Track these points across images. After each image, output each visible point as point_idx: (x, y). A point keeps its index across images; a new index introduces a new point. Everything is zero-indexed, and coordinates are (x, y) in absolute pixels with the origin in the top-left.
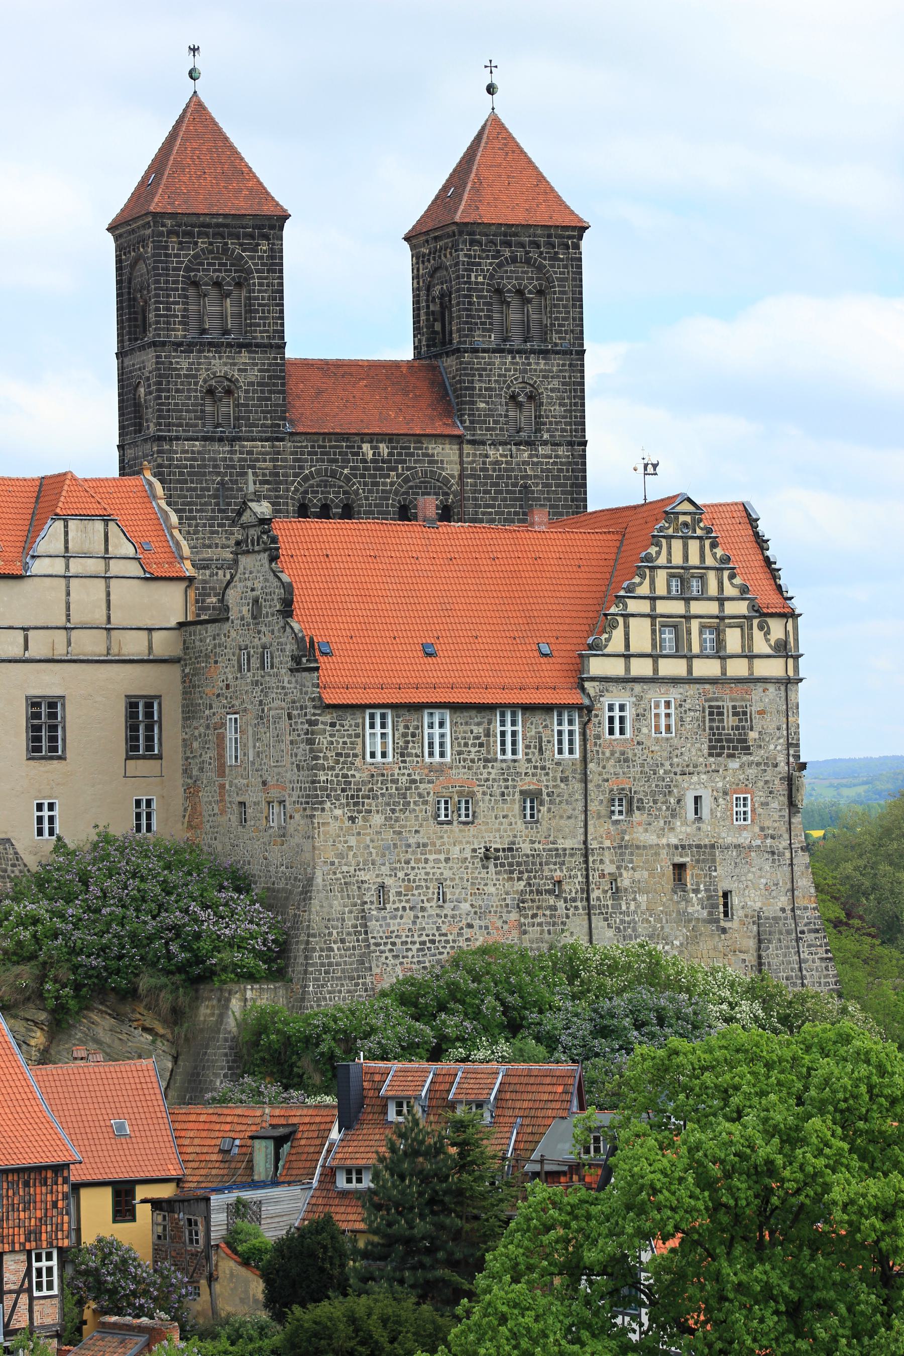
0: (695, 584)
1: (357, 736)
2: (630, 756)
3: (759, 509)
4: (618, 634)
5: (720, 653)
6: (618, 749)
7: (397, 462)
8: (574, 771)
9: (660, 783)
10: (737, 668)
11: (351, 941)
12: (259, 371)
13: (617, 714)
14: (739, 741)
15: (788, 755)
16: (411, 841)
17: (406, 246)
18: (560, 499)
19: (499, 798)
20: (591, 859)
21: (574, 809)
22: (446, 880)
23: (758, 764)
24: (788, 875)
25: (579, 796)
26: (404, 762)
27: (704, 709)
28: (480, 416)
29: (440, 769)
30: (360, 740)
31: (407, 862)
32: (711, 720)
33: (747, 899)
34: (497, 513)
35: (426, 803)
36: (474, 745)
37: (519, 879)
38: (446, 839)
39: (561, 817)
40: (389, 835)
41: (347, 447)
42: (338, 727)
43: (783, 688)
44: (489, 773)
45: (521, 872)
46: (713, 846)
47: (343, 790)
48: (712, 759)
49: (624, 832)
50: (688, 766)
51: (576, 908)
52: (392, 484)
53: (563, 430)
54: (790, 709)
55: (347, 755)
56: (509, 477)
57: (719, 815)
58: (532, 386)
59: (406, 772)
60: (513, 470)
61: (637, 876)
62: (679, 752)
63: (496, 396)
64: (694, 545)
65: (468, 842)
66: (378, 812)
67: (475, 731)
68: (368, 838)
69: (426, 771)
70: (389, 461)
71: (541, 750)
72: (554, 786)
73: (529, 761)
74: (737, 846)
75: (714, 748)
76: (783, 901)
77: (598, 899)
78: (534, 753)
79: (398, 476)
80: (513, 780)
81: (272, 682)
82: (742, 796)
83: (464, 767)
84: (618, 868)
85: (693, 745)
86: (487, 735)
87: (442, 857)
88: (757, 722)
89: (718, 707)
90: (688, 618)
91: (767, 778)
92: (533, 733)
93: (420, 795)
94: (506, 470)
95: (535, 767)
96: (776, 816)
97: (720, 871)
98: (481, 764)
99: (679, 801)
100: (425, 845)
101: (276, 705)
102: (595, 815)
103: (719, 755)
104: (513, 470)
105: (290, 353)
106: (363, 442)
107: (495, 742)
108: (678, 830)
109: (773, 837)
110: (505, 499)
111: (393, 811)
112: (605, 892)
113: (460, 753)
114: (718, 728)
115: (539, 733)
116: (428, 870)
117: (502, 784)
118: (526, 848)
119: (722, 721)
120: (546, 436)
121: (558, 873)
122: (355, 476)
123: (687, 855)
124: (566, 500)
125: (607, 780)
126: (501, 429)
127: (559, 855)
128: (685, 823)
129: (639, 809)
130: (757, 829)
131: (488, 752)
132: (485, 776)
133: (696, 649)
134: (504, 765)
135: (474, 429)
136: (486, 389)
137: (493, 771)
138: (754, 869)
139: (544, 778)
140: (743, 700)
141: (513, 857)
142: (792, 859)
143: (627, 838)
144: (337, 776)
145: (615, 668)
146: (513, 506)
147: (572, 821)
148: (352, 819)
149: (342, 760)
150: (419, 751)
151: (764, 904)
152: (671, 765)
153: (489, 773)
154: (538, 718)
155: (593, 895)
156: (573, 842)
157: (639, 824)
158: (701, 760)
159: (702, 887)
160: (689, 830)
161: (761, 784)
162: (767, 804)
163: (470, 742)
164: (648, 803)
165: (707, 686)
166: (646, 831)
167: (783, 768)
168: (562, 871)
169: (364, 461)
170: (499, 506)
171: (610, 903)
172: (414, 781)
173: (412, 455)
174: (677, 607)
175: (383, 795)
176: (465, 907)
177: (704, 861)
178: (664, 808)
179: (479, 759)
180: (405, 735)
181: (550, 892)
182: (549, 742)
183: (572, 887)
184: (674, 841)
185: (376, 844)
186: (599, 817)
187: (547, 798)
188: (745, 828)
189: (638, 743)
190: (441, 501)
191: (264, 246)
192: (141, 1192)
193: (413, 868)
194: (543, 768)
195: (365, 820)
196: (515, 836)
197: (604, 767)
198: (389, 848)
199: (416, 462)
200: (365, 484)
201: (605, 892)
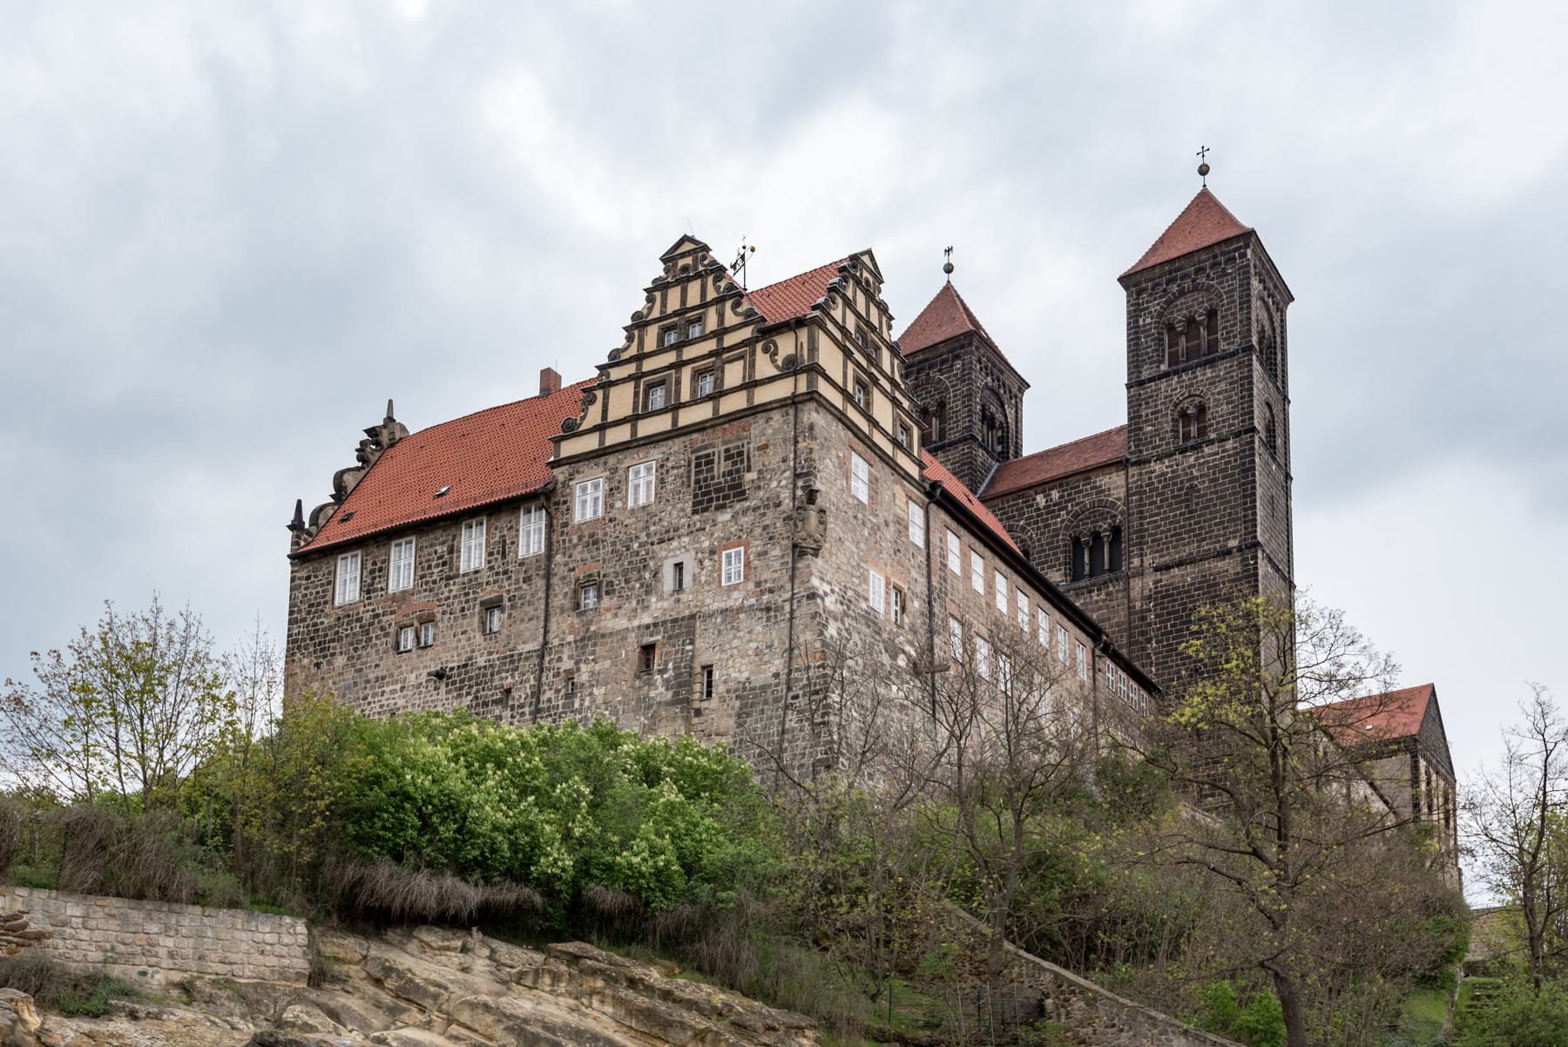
1: (329, 583)
2: (600, 536)
6: (586, 533)
7: (1066, 502)
8: (538, 568)
9: (633, 559)
12: (951, 464)
14: (731, 488)
15: (795, 487)
16: (371, 676)
18: (1227, 489)
19: (459, 614)
20: (547, 658)
21: (536, 610)
22: (398, 709)
23: (755, 509)
24: (786, 631)
25: (542, 594)
26: (369, 598)
27: (690, 462)
28: (1146, 438)
30: (330, 587)
31: (365, 698)
32: (697, 473)
33: (731, 671)
34: (1162, 520)
35: (387, 635)
36: (437, 566)
37: (468, 694)
38: (404, 668)
39: (522, 620)
40: (350, 675)
41: (1023, 503)
42: (312, 579)
43: (791, 412)
44: (451, 591)
45: (470, 687)
46: (693, 617)
47: (312, 639)
48: (697, 517)
49: (590, 623)
50: (667, 532)
51: (523, 714)
52: (1062, 522)
53: (1230, 426)
55: (319, 604)
56: (1174, 484)
57: (703, 579)
58: (1199, 396)
59: (370, 608)
60: (1178, 476)
61: (597, 667)
62: (657, 519)
63: (1162, 417)
65: (425, 667)
66: (341, 653)
67: (439, 551)
68: (331, 681)
69: (389, 603)
70: (1060, 503)
71: (504, 555)
72: (516, 589)
73: (491, 568)
74: (723, 612)
75: (701, 503)
76: (778, 664)
77: (549, 700)
78: (496, 559)
79: (1068, 514)
80: (474, 592)
82: (733, 551)
83: (426, 590)
84: (577, 663)
85: (674, 506)
86: (451, 551)
87: (398, 687)
88: (757, 462)
89: (708, 455)
91: (765, 523)
92: (497, 539)
93: (382, 629)
94: (1171, 478)
95: (497, 574)
96: (777, 565)
97: (699, 643)
98: (443, 583)
99: (655, 576)
100: (383, 678)
102: (558, 611)
103: (705, 510)
104: (1178, 476)
106: (1037, 494)
107: (459, 557)
108: (653, 607)
109: (771, 591)
110: (1171, 504)
111: (356, 650)
112: (558, 691)
113: (422, 577)
114: (706, 479)
115: (504, 536)
116: (384, 702)
117: (463, 599)
118: (481, 662)
119: (712, 470)
120: (1213, 436)
121: (510, 680)
122: (1029, 525)
123: (658, 633)
124: (1234, 487)
125: (573, 569)
126: (1167, 444)
127: (512, 661)
128: (661, 598)
129: (608, 593)
130: (751, 586)
131: (451, 569)
132: (446, 594)
134: (466, 579)
135: (1141, 451)
136: (1152, 413)
137: (454, 588)
138: (741, 634)
139: (506, 583)
140: (739, 439)
141: (466, 673)
142: (792, 612)
143: (593, 628)
144: (308, 626)
146: (1178, 509)
147: (534, 622)
148: (318, 665)
149: (313, 610)
150: (383, 585)
151: (752, 673)
152: (648, 535)
153: (451, 591)
155: (544, 698)
156: (534, 646)
157: (608, 610)
158: (683, 520)
159: (670, 665)
160: (666, 604)
161: (758, 531)
162: (766, 553)
163: (433, 564)
164: (619, 583)
165: (695, 436)
166: (616, 615)
168: (513, 676)
169: (1039, 509)
170: (1165, 512)
171: (560, 703)
172: (377, 616)
173: (1081, 491)
175: (347, 636)
177: (678, 636)
178: (638, 585)
179: (441, 579)
180: (372, 572)
181: (496, 702)
182: (513, 543)
183: (521, 695)
184: (647, 619)
185: (338, 686)
186: (562, 612)
187: (508, 604)
188: (736, 587)
189: (611, 520)
190: (1109, 524)
193: (369, 703)
194: (505, 572)
195: (329, 663)
196: (473, 651)
197: (570, 556)
198: (349, 687)
199: (1084, 496)
200: (1038, 528)
201: (558, 691)
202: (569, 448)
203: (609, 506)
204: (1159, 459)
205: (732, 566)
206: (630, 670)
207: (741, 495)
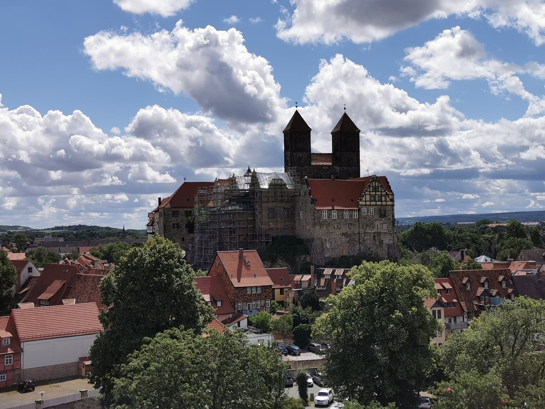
0: (377, 190)
3: (387, 177)
4: (364, 198)
5: (381, 201)
10: (384, 203)
11: (320, 248)
13: (364, 211)
17: (331, 135)
29: (335, 220)
40: (326, 231)
54: (393, 210)
64: (377, 183)
76: (392, 242)
81: (308, 206)
90: (376, 195)
101: (308, 209)
105: (312, 152)
133: (377, 200)
145: (364, 203)
154: (351, 211)
155: (361, 240)
156: (357, 232)
164: (369, 225)
167: (392, 220)
174: (374, 193)
176: (339, 243)
191: (308, 135)
192: (285, 290)
202: (361, 203)
203: (367, 214)
204: (345, 167)
205: (385, 226)
206: (373, 239)
207: (386, 217)
